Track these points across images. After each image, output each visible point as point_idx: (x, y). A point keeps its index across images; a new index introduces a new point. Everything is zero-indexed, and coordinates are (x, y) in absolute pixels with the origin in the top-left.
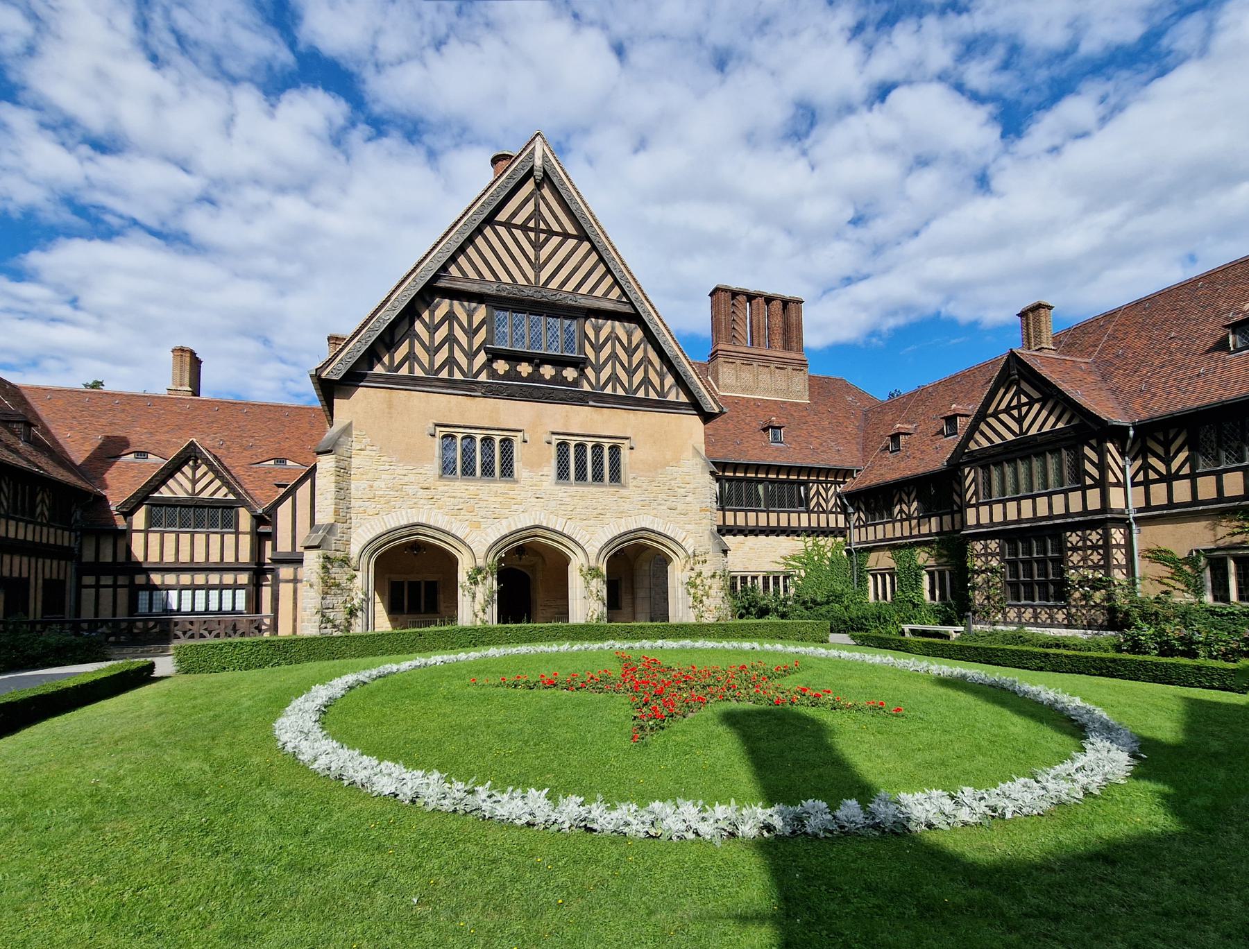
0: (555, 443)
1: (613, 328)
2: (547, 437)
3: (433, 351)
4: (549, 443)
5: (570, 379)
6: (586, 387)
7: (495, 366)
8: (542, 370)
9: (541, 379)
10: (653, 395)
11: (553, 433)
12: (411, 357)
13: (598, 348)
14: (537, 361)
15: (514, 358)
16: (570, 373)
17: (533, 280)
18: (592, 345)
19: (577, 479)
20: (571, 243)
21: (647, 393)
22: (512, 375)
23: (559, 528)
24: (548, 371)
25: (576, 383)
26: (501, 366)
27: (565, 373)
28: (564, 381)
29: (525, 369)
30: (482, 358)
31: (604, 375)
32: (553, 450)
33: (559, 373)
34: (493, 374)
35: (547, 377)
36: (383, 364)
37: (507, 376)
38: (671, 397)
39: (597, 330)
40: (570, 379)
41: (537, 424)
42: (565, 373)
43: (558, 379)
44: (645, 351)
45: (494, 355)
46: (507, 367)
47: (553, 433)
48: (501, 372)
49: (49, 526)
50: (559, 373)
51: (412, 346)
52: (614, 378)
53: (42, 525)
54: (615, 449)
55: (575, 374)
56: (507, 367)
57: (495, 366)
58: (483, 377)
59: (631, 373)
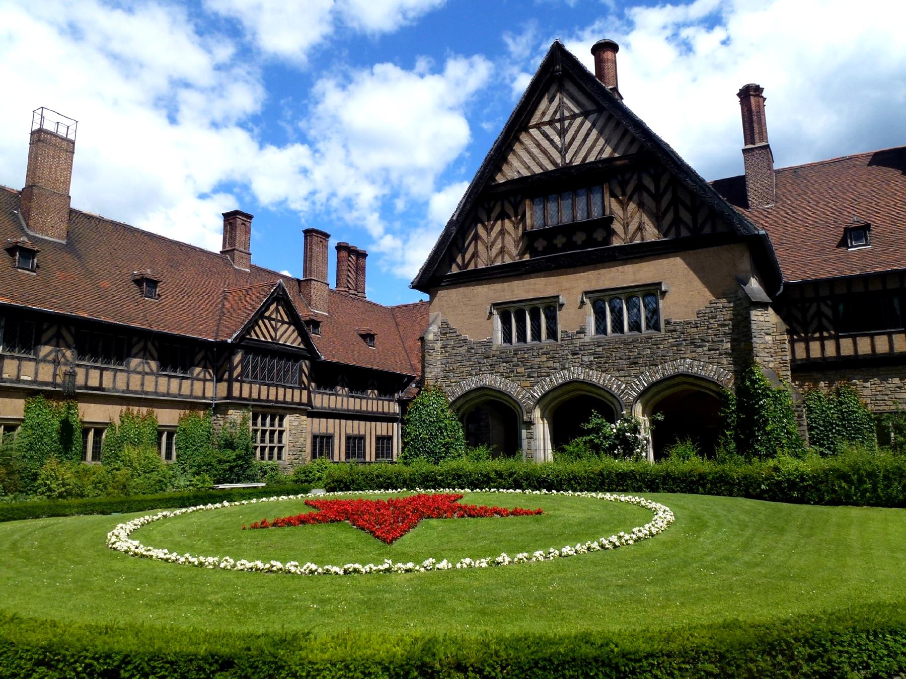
1: (640, 179)
3: (489, 247)
5: (600, 239)
6: (616, 242)
8: (575, 238)
10: (684, 233)
12: (475, 255)
15: (547, 234)
17: (559, 161)
20: (579, 120)
21: (678, 233)
36: (458, 265)
37: (546, 251)
38: (707, 230)
40: (600, 239)
41: (571, 288)
49: (378, 400)
51: (476, 247)
52: (640, 228)
53: (373, 399)
56: (545, 243)
57: (536, 245)
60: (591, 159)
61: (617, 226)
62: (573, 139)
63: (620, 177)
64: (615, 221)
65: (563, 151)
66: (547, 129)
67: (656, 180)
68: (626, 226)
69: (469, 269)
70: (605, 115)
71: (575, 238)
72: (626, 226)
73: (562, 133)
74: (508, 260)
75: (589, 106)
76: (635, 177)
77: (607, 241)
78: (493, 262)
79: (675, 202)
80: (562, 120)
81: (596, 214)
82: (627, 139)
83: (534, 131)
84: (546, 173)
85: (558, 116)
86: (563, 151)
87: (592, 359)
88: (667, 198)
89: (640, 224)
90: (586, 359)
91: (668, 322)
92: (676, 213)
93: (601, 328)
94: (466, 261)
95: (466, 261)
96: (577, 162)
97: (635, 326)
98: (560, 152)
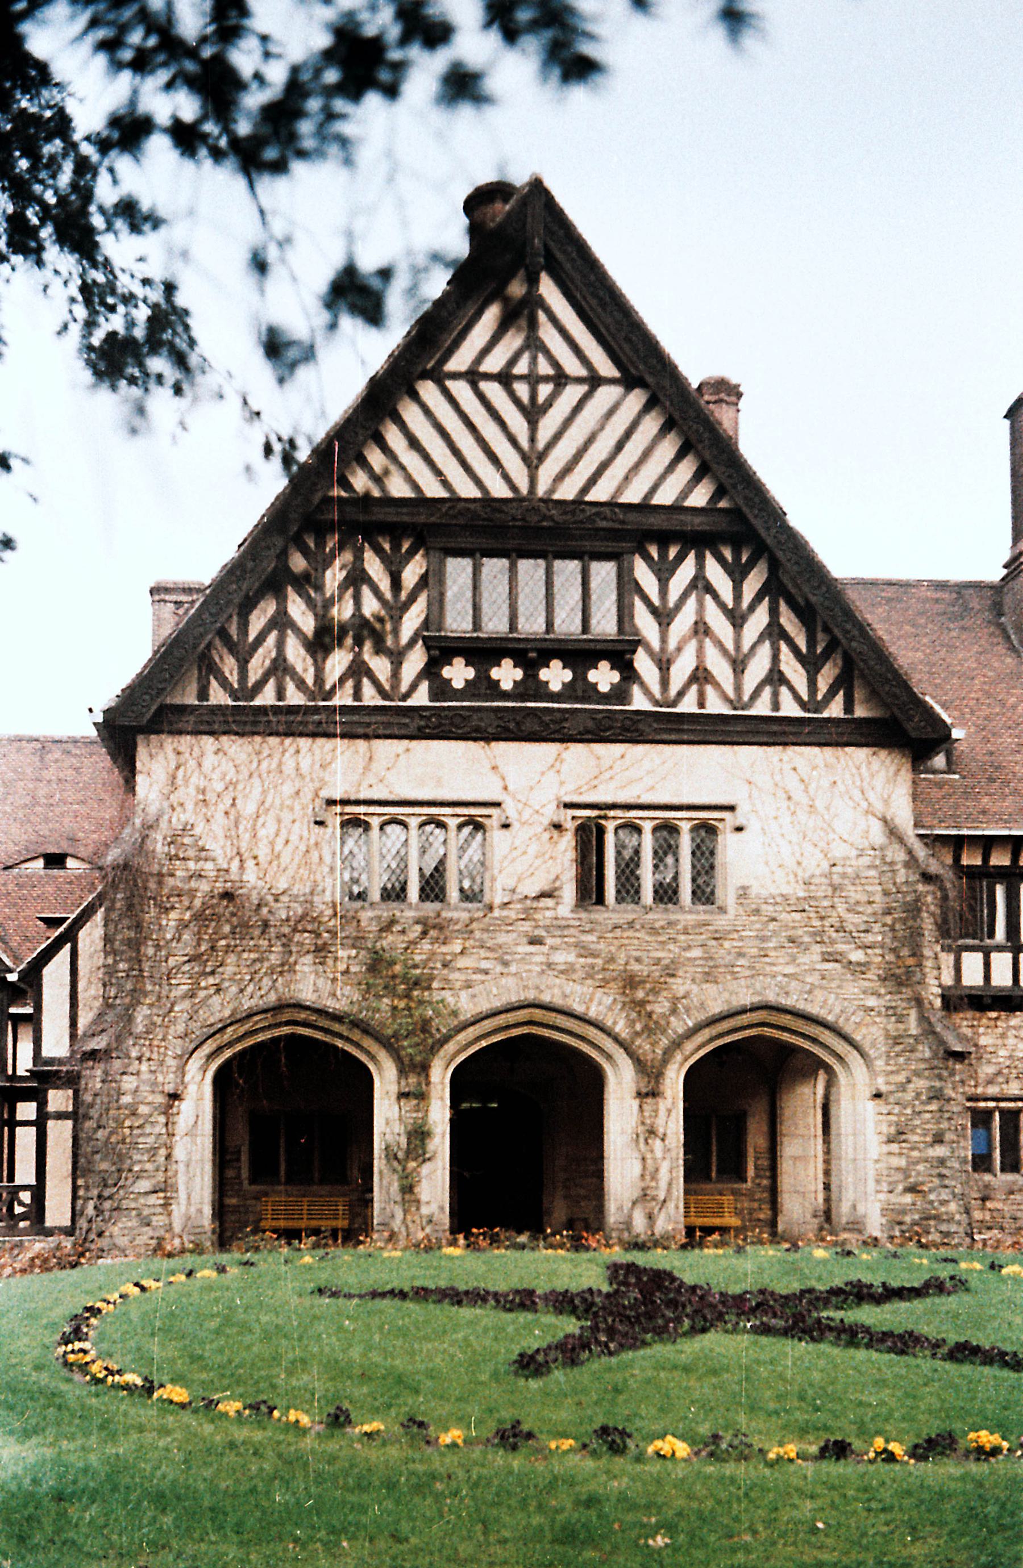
0: (570, 826)
2: (551, 813)
4: (558, 827)
5: (604, 688)
6: (639, 702)
7: (446, 672)
9: (541, 691)
10: (790, 709)
11: (568, 806)
13: (663, 616)
14: (531, 655)
15: (483, 652)
16: (604, 677)
18: (654, 611)
19: (620, 900)
21: (776, 706)
22: (483, 686)
23: (579, 1008)
24: (556, 675)
25: (620, 694)
26: (458, 673)
27: (592, 676)
28: (590, 692)
29: (507, 674)
30: (416, 661)
31: (681, 670)
32: (568, 842)
33: (580, 677)
34: (441, 689)
35: (555, 687)
37: (471, 689)
38: (835, 710)
39: (664, 573)
40: (604, 688)
42: (592, 676)
43: (580, 689)
44: (774, 612)
45: (441, 650)
46: (470, 673)
47: (568, 806)
48: (458, 684)
50: (580, 677)
51: (280, 645)
52: (701, 676)
54: (707, 830)
55: (615, 677)
57: (446, 672)
58: (421, 698)
59: (739, 665)
60: (600, 493)
61: (642, 662)
62: (557, 437)
63: (654, 551)
64: (640, 651)
65: (533, 460)
66: (493, 390)
67: (737, 574)
68: (664, 665)
69: (258, 702)
70: (636, 400)
71: (544, 674)
72: (664, 665)
73: (533, 412)
74: (370, 697)
75: (606, 368)
76: (690, 560)
77: (620, 694)
78: (329, 695)
79: (774, 632)
80: (533, 380)
81: (605, 624)
82: (686, 469)
83: (461, 389)
84: (488, 501)
85: (521, 368)
86: (533, 460)
87: (571, 958)
88: (759, 619)
89: (697, 668)
90: (560, 958)
91: (743, 893)
92: (775, 658)
93: (590, 891)
94: (253, 678)
95: (253, 678)
96: (568, 491)
97: (666, 894)
98: (525, 458)
